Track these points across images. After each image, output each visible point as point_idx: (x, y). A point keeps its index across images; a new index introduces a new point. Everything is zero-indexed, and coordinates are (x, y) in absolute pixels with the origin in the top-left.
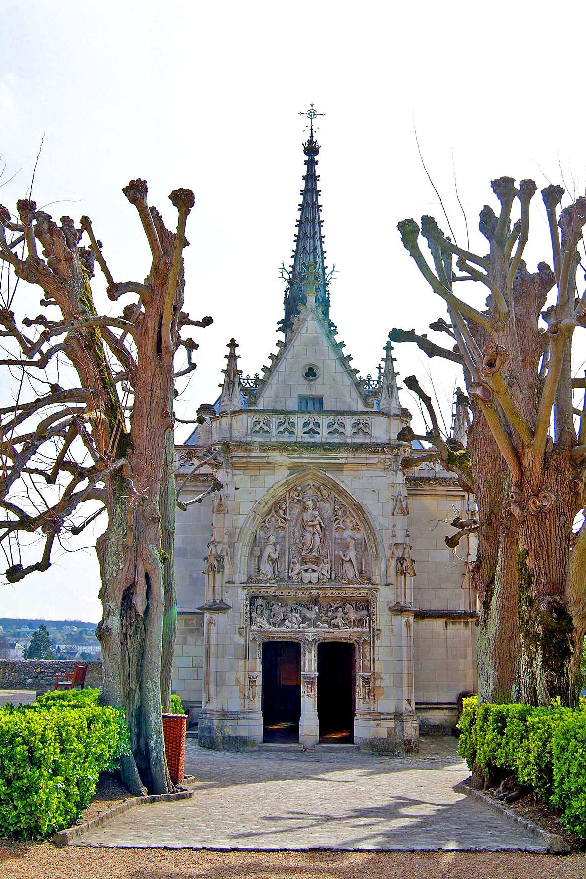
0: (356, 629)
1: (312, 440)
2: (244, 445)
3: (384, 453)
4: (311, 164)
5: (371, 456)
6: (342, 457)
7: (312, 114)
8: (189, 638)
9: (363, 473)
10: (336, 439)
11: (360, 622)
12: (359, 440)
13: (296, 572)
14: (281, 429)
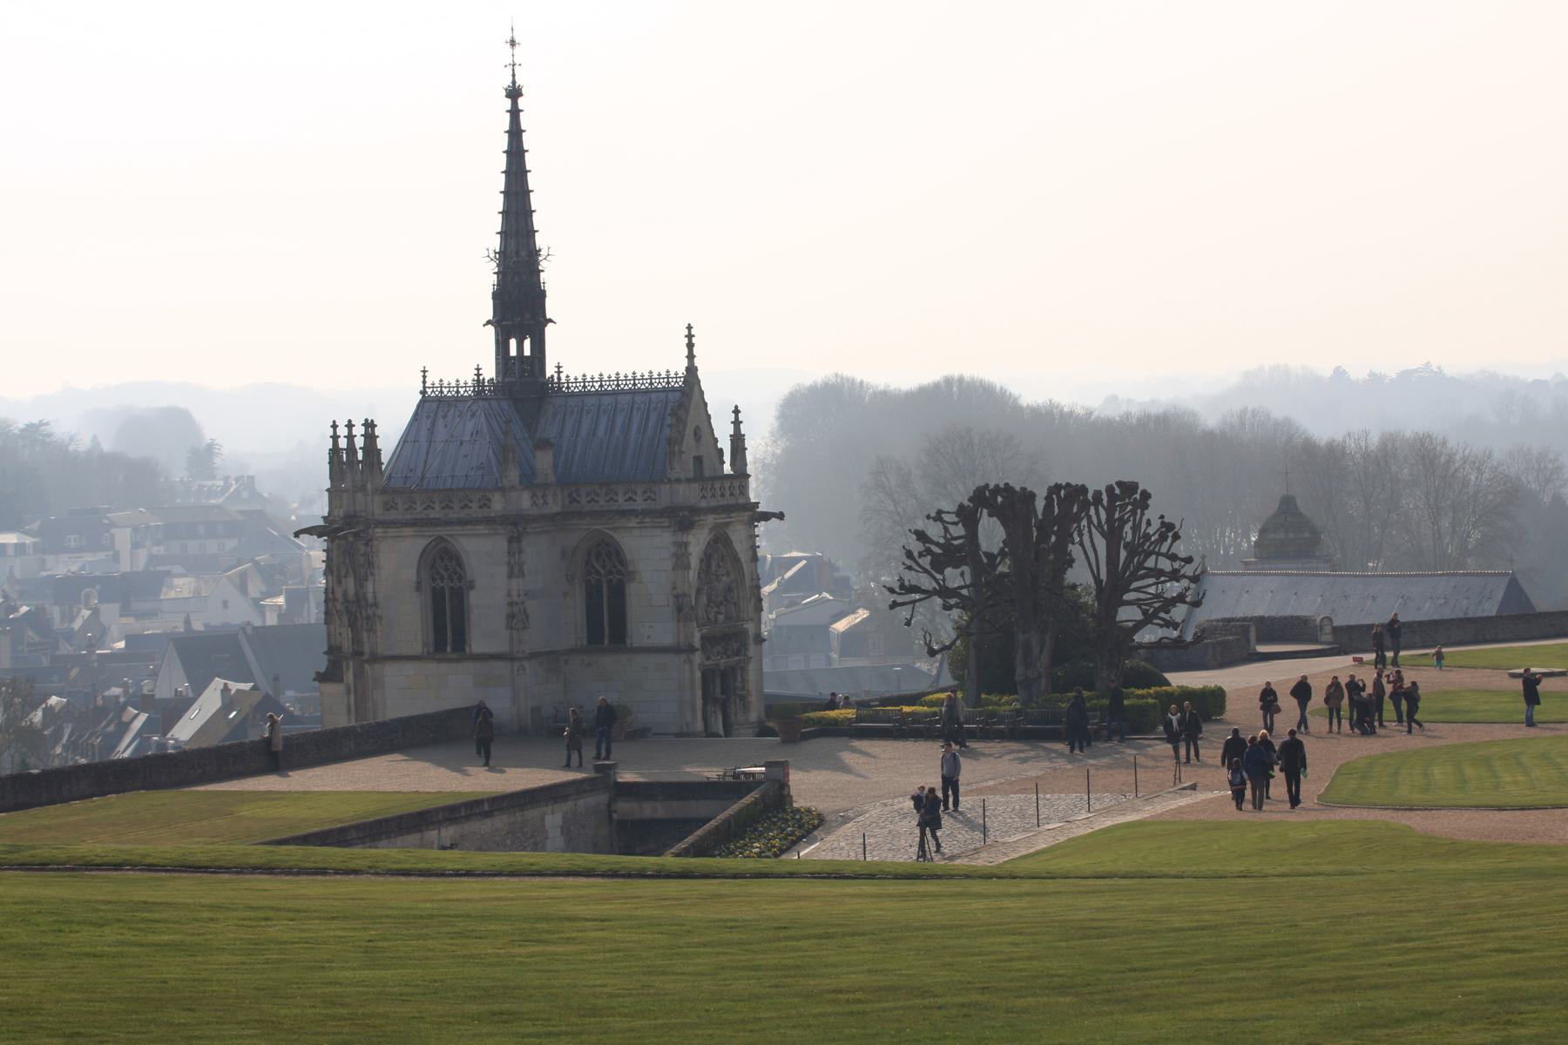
4: (515, 113)
7: (513, 43)
11: (738, 653)
12: (741, 501)
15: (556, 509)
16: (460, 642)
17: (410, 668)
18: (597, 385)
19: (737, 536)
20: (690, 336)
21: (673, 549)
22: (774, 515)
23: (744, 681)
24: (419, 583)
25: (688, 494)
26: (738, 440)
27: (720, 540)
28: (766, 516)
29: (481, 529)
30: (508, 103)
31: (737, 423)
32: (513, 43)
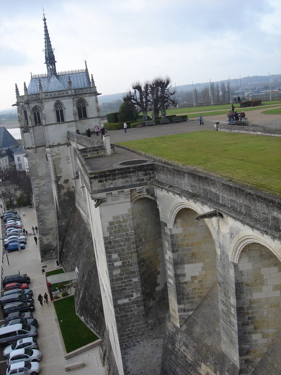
4: (45, 23)
16: (63, 120)
17: (54, 126)
18: (68, 73)
20: (86, 63)
21: (95, 99)
29: (67, 98)
30: (44, 22)
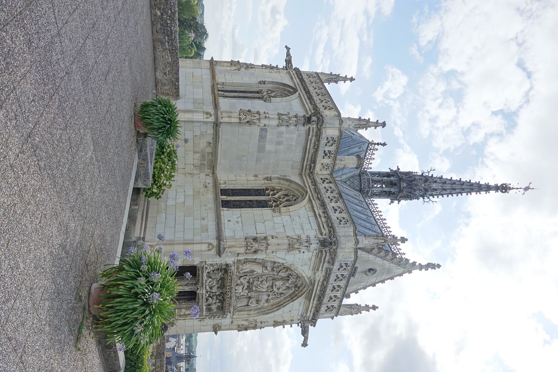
0: (204, 308)
1: (328, 290)
2: (332, 261)
3: (312, 319)
5: (312, 314)
6: (314, 302)
7: (527, 189)
8: (198, 155)
9: (302, 307)
10: (326, 300)
11: (209, 310)
12: (324, 308)
13: (243, 282)
14: (340, 276)
15: (318, 167)
18: (378, 217)
19: (297, 307)
21: (304, 237)
22: (306, 339)
23: (185, 315)
24: (264, 83)
25: (345, 252)
26: (356, 309)
27: (297, 287)
28: (305, 332)
31: (367, 308)
32: (527, 189)
